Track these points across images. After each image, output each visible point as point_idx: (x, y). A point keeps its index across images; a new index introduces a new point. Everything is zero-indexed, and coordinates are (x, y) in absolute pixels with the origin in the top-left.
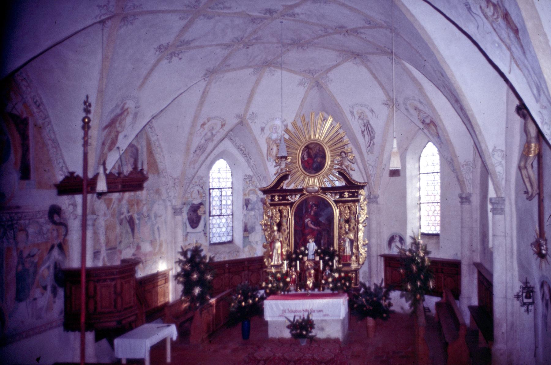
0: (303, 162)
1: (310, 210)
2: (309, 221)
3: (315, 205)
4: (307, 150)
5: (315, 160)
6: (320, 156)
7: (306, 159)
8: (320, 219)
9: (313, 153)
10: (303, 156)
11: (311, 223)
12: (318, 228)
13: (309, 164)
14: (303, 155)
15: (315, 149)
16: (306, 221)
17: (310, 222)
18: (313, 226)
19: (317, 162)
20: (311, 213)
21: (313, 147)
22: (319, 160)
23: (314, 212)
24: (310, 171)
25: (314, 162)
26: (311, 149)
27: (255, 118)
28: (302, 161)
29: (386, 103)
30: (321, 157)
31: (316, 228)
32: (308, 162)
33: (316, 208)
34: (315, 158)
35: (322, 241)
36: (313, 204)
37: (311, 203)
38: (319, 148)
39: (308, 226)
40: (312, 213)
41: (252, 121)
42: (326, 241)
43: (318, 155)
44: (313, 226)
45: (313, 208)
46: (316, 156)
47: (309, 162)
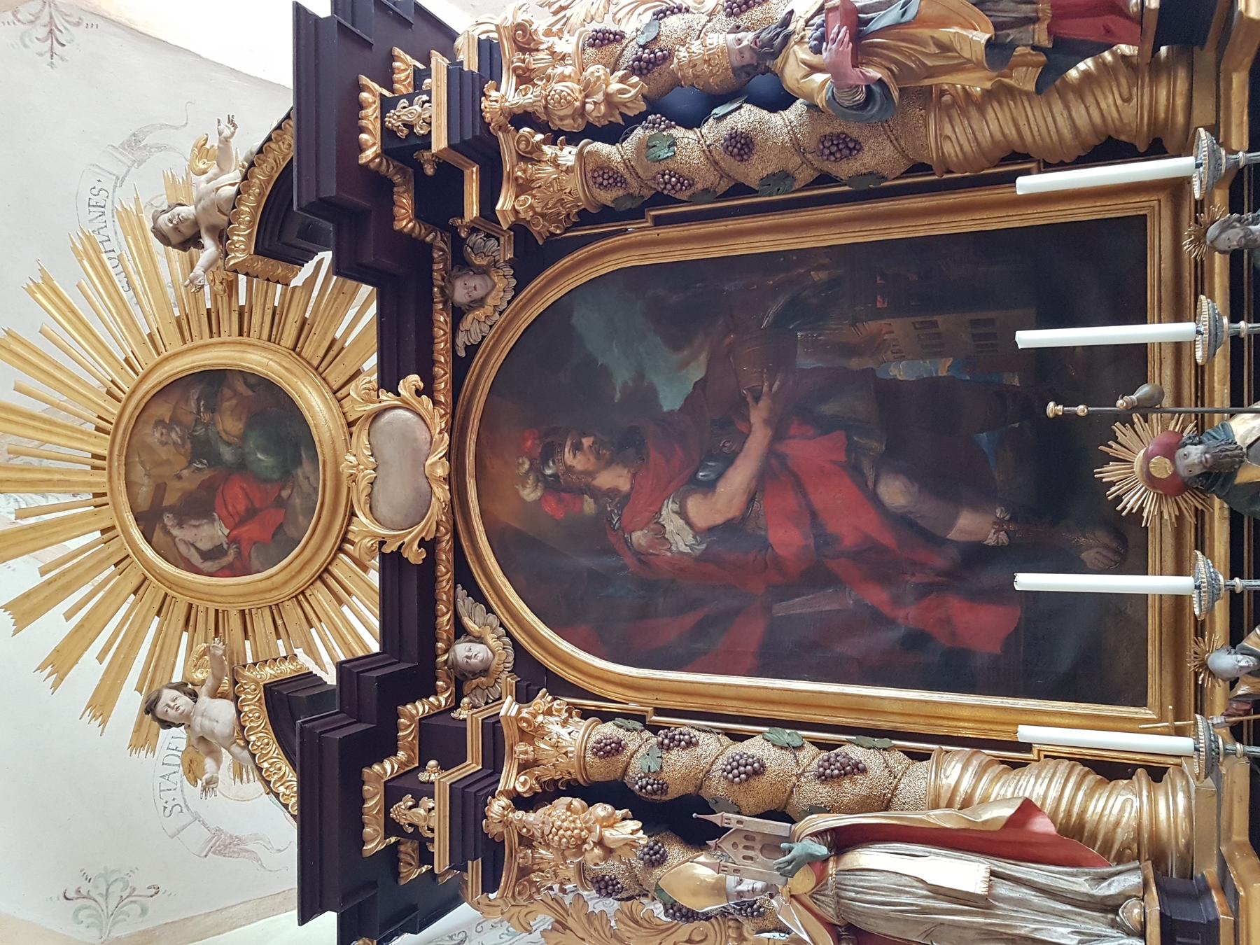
0: (239, 553)
1: (589, 506)
2: (683, 514)
3: (550, 452)
4: (168, 520)
5: (227, 454)
6: (206, 417)
7: (213, 532)
8: (671, 399)
9: (189, 479)
10: (206, 555)
11: (709, 487)
12: (757, 415)
13: (251, 513)
14: (196, 559)
15: (164, 453)
16: (681, 540)
17: (695, 505)
18: (738, 479)
19: (243, 437)
20: (613, 493)
21: (148, 475)
22: (230, 425)
23: (609, 464)
24: (297, 501)
25: (242, 465)
26: (160, 489)
27: (116, 889)
28: (231, 571)
29: (42, 32)
30: (212, 409)
31: (758, 439)
32: (242, 521)
33: (577, 447)
34: (214, 459)
35: (899, 371)
36: (536, 469)
37: (530, 493)
38: (159, 422)
39: (731, 528)
40: (615, 479)
41: (136, 909)
42: (898, 328)
43: (200, 431)
44: (738, 479)
45: (569, 469)
46: (202, 450)
47: (241, 508)
